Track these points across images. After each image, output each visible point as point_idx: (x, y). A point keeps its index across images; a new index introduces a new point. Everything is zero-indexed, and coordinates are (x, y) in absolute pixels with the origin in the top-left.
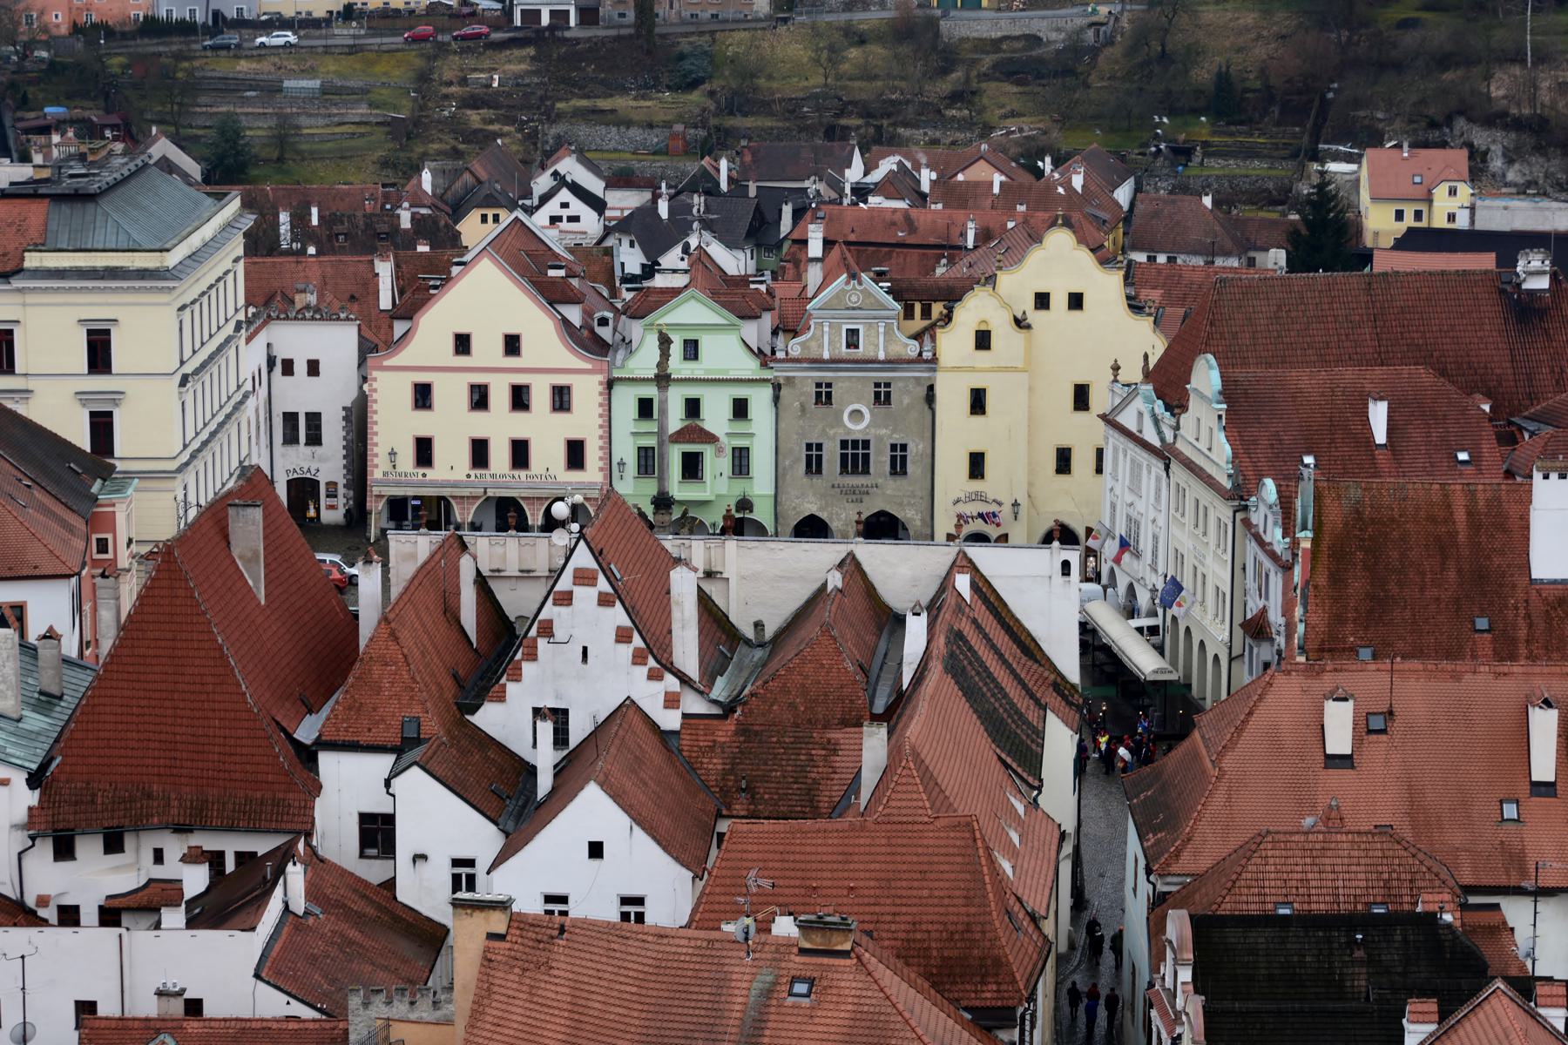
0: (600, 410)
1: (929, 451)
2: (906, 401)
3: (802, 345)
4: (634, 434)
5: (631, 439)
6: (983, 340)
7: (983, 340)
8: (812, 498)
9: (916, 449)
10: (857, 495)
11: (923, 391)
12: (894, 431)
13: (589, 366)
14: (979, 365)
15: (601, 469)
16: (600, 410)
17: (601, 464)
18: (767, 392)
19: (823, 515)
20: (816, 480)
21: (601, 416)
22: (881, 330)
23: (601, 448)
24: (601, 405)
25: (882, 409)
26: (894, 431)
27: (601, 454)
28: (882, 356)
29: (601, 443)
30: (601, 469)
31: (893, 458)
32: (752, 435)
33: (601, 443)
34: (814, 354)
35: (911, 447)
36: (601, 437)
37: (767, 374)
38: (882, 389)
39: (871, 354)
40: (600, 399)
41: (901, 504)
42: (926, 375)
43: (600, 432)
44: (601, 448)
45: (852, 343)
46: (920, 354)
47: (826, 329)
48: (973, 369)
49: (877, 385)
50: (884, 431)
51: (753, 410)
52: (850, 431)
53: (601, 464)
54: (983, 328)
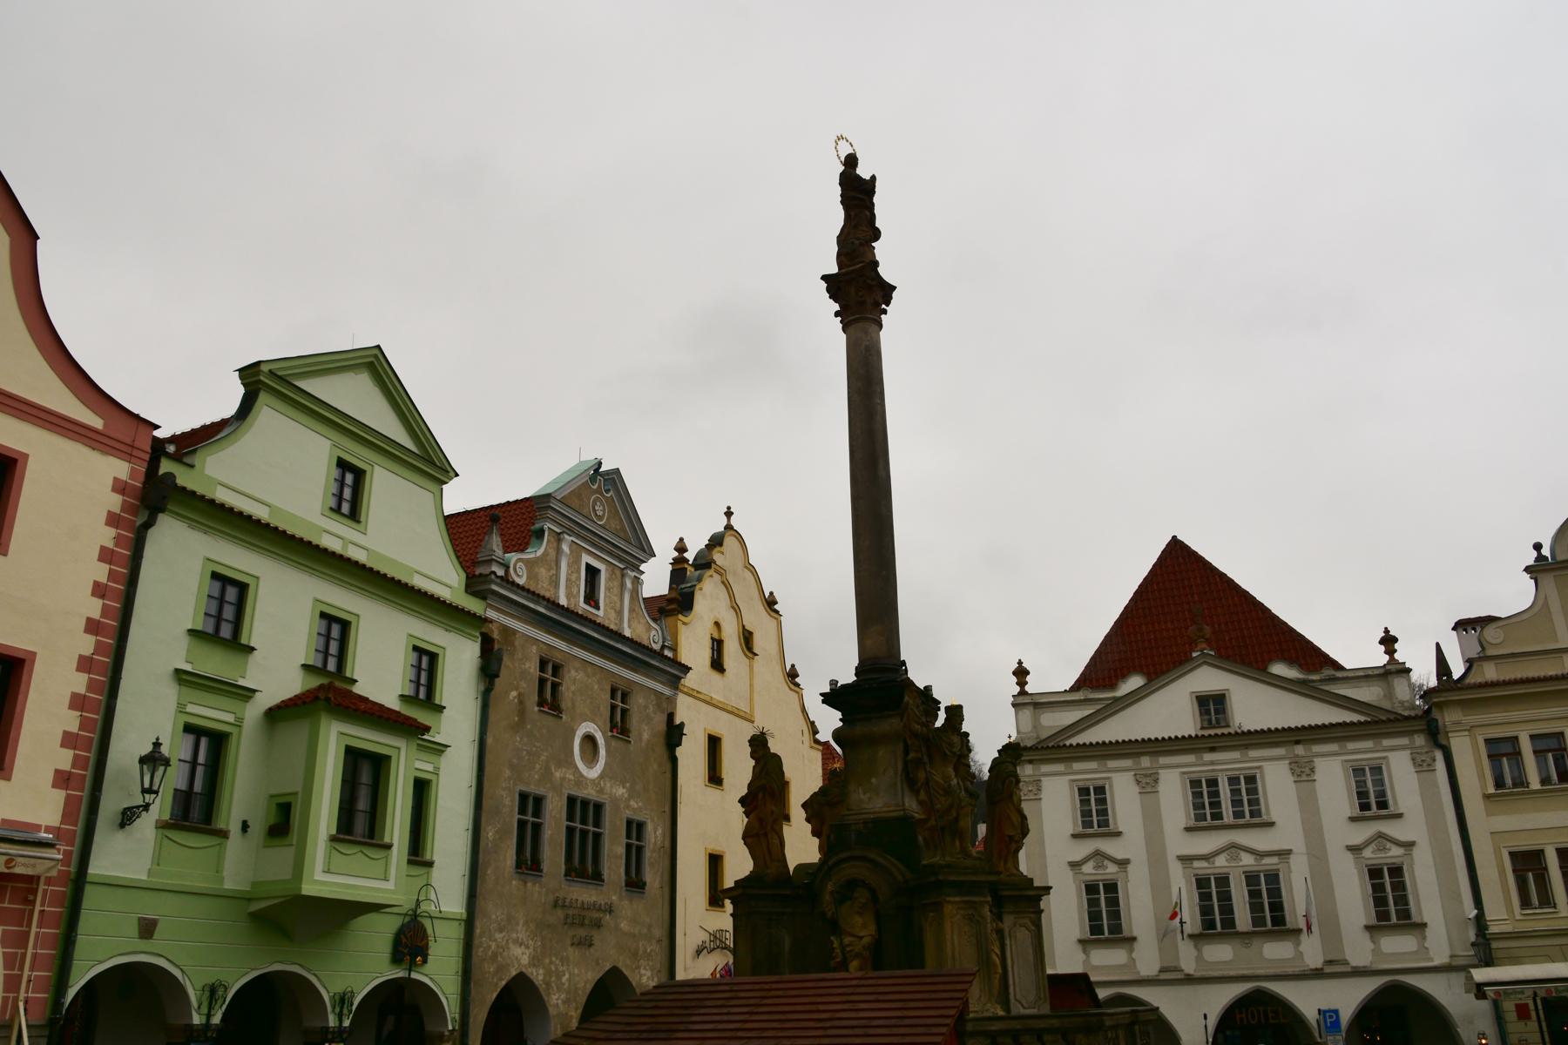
0: (101, 572)
1: (667, 844)
2: (646, 736)
3: (529, 564)
4: (181, 676)
5: (170, 693)
8: (521, 933)
9: (655, 834)
10: (583, 925)
11: (660, 722)
12: (631, 797)
13: (96, 422)
15: (62, 779)
16: (101, 572)
17: (64, 759)
19: (537, 976)
20: (533, 888)
21: (99, 590)
22: (629, 584)
23: (77, 702)
24: (105, 555)
26: (631, 797)
27: (71, 721)
28: (627, 633)
29: (80, 683)
30: (62, 779)
31: (629, 846)
32: (439, 749)
33: (80, 683)
34: (544, 589)
35: (650, 827)
36: (85, 664)
40: (107, 537)
41: (635, 954)
42: (667, 691)
43: (87, 644)
44: (77, 702)
45: (591, 598)
46: (663, 647)
47: (565, 548)
49: (613, 691)
50: (621, 791)
52: (580, 780)
53: (65, 759)
54: (716, 636)
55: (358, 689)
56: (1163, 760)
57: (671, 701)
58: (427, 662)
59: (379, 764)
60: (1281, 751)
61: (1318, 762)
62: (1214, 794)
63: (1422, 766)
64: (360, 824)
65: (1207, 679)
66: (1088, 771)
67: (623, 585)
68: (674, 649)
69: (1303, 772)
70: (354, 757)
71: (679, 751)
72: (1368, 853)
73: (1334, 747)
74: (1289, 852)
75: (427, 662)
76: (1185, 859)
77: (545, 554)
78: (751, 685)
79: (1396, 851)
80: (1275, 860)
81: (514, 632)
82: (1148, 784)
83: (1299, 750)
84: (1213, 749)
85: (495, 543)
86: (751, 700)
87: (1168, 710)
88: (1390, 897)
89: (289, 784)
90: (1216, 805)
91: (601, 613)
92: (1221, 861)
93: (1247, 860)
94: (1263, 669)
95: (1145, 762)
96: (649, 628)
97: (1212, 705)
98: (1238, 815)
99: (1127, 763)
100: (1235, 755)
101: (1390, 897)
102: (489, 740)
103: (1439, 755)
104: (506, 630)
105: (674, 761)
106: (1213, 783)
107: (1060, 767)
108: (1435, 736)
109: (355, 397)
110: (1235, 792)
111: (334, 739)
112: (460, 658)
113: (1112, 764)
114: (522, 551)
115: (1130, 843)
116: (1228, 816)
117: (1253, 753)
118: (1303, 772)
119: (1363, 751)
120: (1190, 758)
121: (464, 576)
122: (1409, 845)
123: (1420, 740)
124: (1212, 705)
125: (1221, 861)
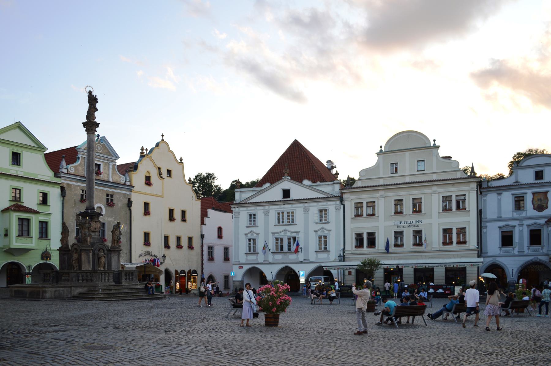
2: (120, 205)
6: (148, 181)
7: (148, 181)
14: (147, 192)
18: (58, 190)
22: (111, 167)
25: (110, 209)
28: (111, 180)
32: (50, 214)
37: (58, 180)
38: (110, 198)
39: (106, 179)
42: (128, 193)
46: (126, 181)
48: (145, 194)
49: (108, 195)
50: (111, 219)
51: (50, 200)
54: (148, 175)
55: (24, 205)
56: (271, 207)
57: (130, 195)
58: (45, 196)
59: (28, 220)
60: (301, 205)
61: (311, 209)
62: (283, 216)
63: (337, 210)
64: (25, 233)
65: (286, 184)
66: (252, 210)
67: (109, 167)
68: (130, 181)
69: (306, 210)
70: (21, 220)
71: (132, 208)
72: (319, 232)
73: (315, 204)
74: (299, 232)
75: (45, 196)
76: (273, 233)
77: (81, 163)
78: (163, 188)
79: (326, 232)
80: (295, 234)
81: (71, 185)
82: (267, 213)
83: (306, 205)
84: (284, 204)
85: (64, 163)
86: (162, 191)
87: (274, 192)
88: (323, 245)
89: (7, 226)
90: (283, 219)
91: (101, 176)
92: (282, 234)
93: (289, 234)
94: (301, 182)
95: (267, 207)
96: (120, 177)
97: (286, 193)
98: (289, 222)
99: (262, 208)
100: (289, 206)
101: (323, 245)
102: (65, 211)
103: (342, 206)
104: (68, 184)
105: (130, 210)
106: (283, 213)
107: (245, 209)
108: (342, 200)
109: (17, 137)
110: (288, 216)
111: (15, 216)
112: (54, 193)
113: (258, 208)
114: (75, 162)
115: (260, 230)
116: (286, 222)
117: (294, 205)
118: (306, 210)
119: (323, 205)
120: (278, 207)
121: (53, 173)
122: (330, 231)
123: (338, 202)
124: (286, 193)
125: (282, 234)
